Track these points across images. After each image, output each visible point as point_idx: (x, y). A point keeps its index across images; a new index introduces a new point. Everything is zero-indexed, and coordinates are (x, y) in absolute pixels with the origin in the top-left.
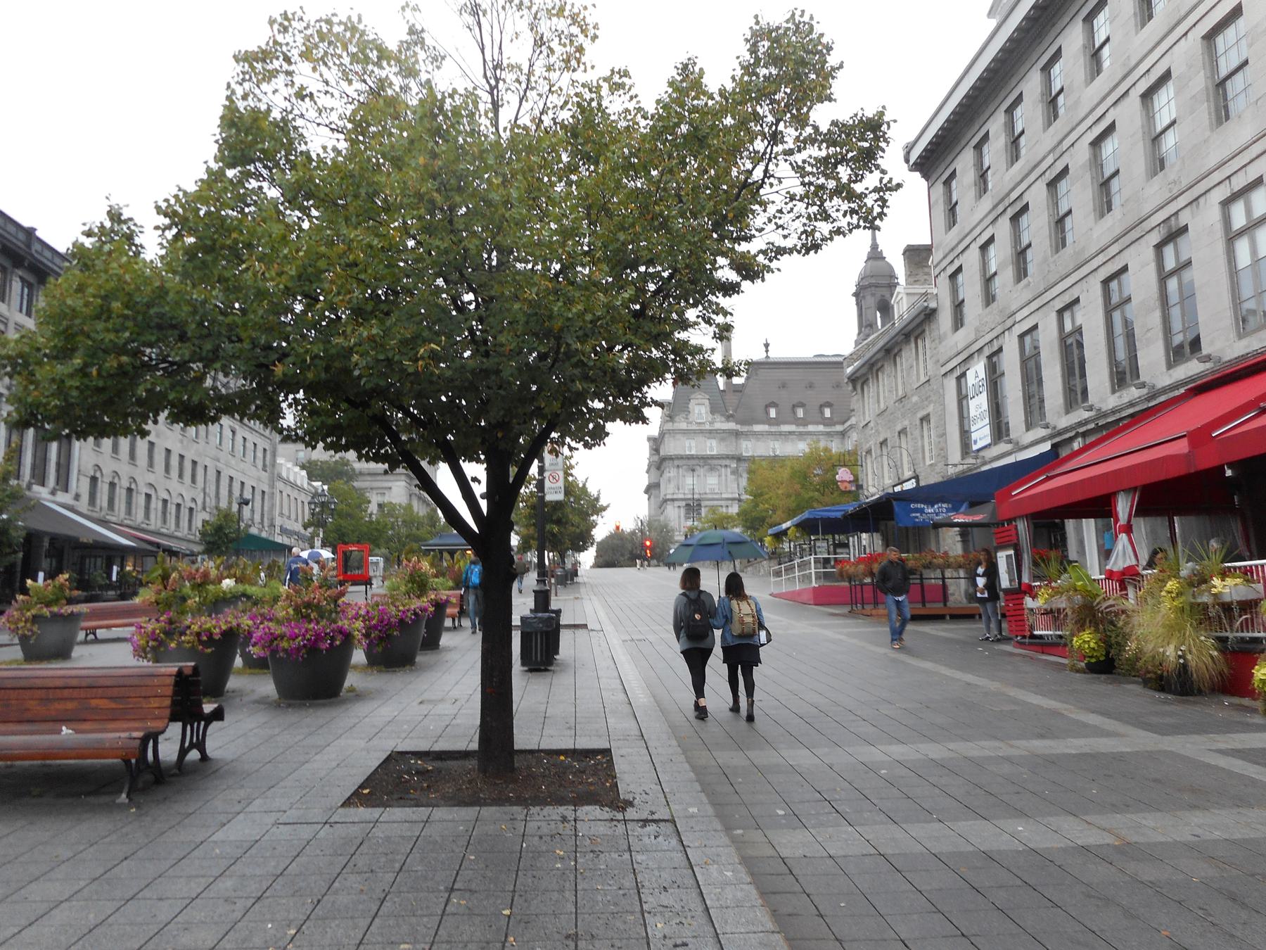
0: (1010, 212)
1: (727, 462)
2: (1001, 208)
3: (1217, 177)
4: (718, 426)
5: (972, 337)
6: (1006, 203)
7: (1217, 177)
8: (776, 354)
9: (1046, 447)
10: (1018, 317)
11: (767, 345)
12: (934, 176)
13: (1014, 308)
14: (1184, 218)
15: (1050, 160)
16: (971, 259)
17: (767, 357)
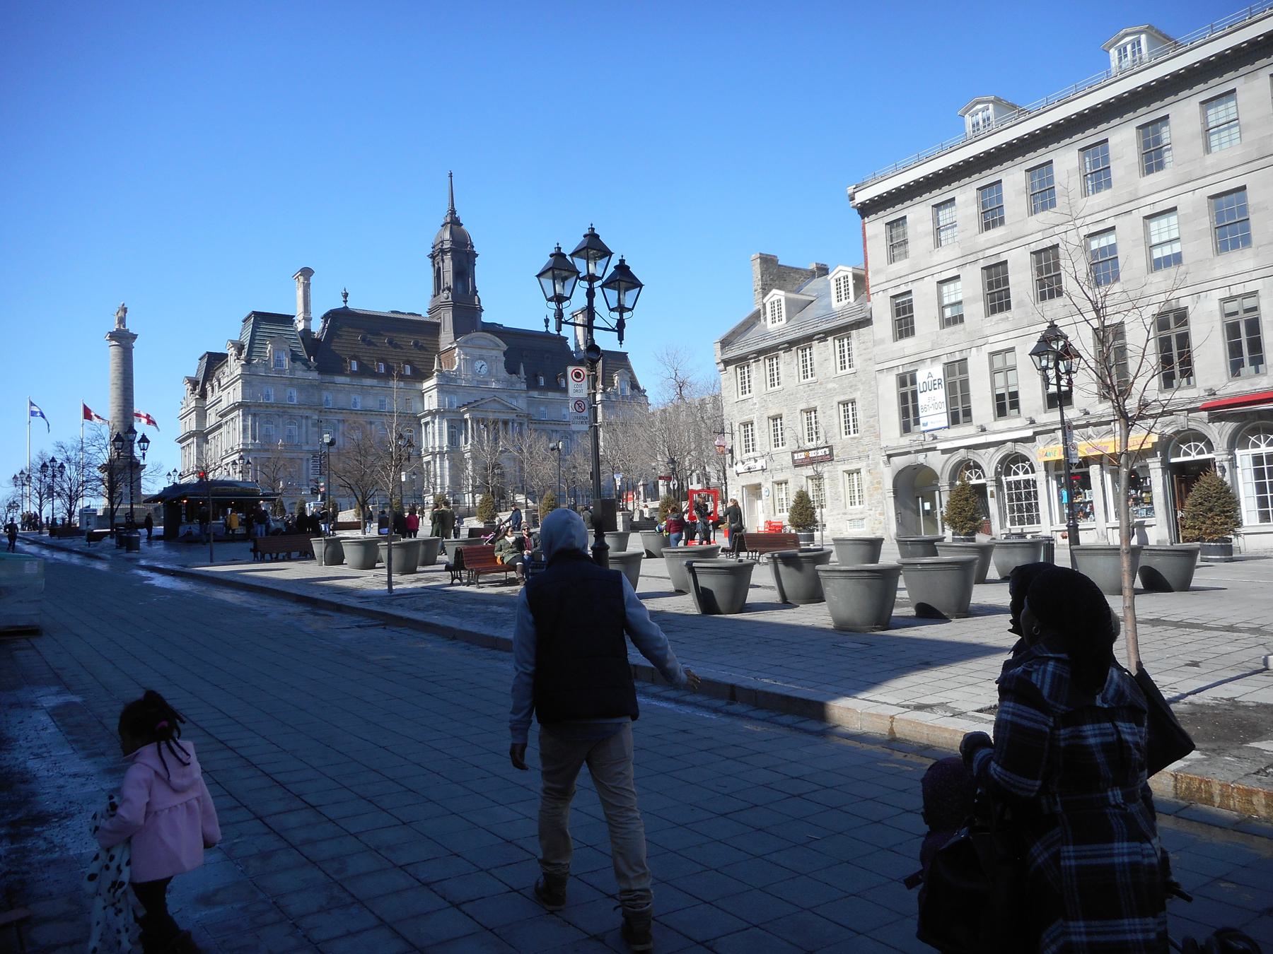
0: (983, 263)
1: (308, 413)
2: (971, 258)
3: (1219, 283)
4: (299, 374)
5: (928, 346)
6: (980, 255)
7: (1219, 283)
8: (355, 304)
9: (1029, 433)
10: (991, 339)
11: (346, 295)
12: (873, 217)
13: (987, 332)
14: (1183, 303)
15: (1039, 236)
17: (346, 308)
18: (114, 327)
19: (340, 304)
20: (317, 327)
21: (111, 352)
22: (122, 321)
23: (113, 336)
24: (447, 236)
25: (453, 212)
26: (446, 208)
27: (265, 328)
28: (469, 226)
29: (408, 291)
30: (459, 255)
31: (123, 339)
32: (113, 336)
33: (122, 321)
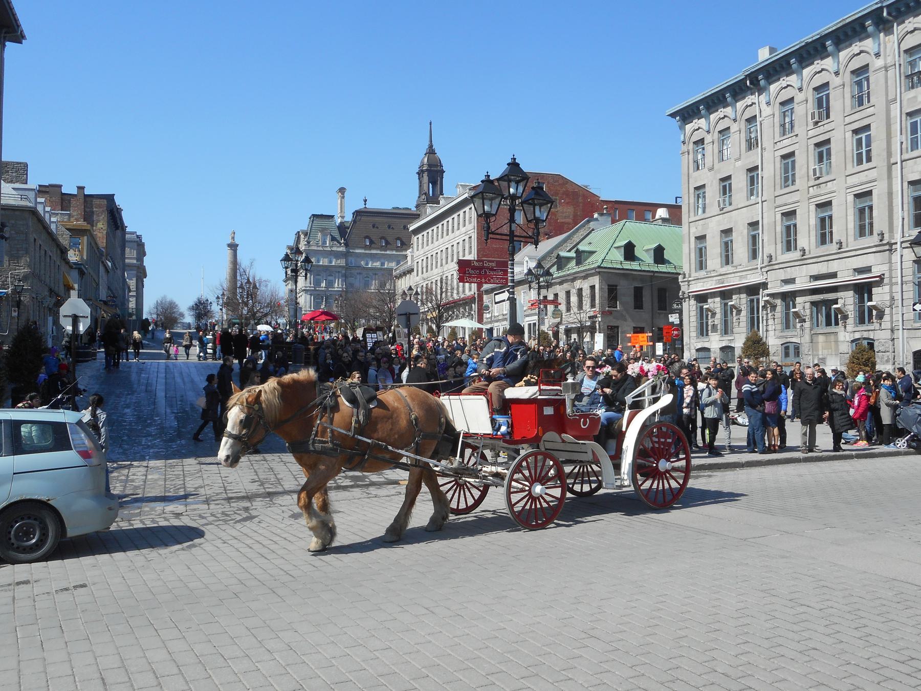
4: (334, 249)
11: (365, 201)
16: (420, 261)
18: (230, 241)
19: (360, 206)
20: (349, 218)
21: (228, 252)
22: (233, 238)
23: (229, 245)
24: (426, 160)
25: (431, 146)
26: (428, 143)
27: (318, 222)
28: (440, 154)
29: (404, 195)
30: (433, 173)
31: (233, 247)
32: (229, 245)
33: (233, 238)
